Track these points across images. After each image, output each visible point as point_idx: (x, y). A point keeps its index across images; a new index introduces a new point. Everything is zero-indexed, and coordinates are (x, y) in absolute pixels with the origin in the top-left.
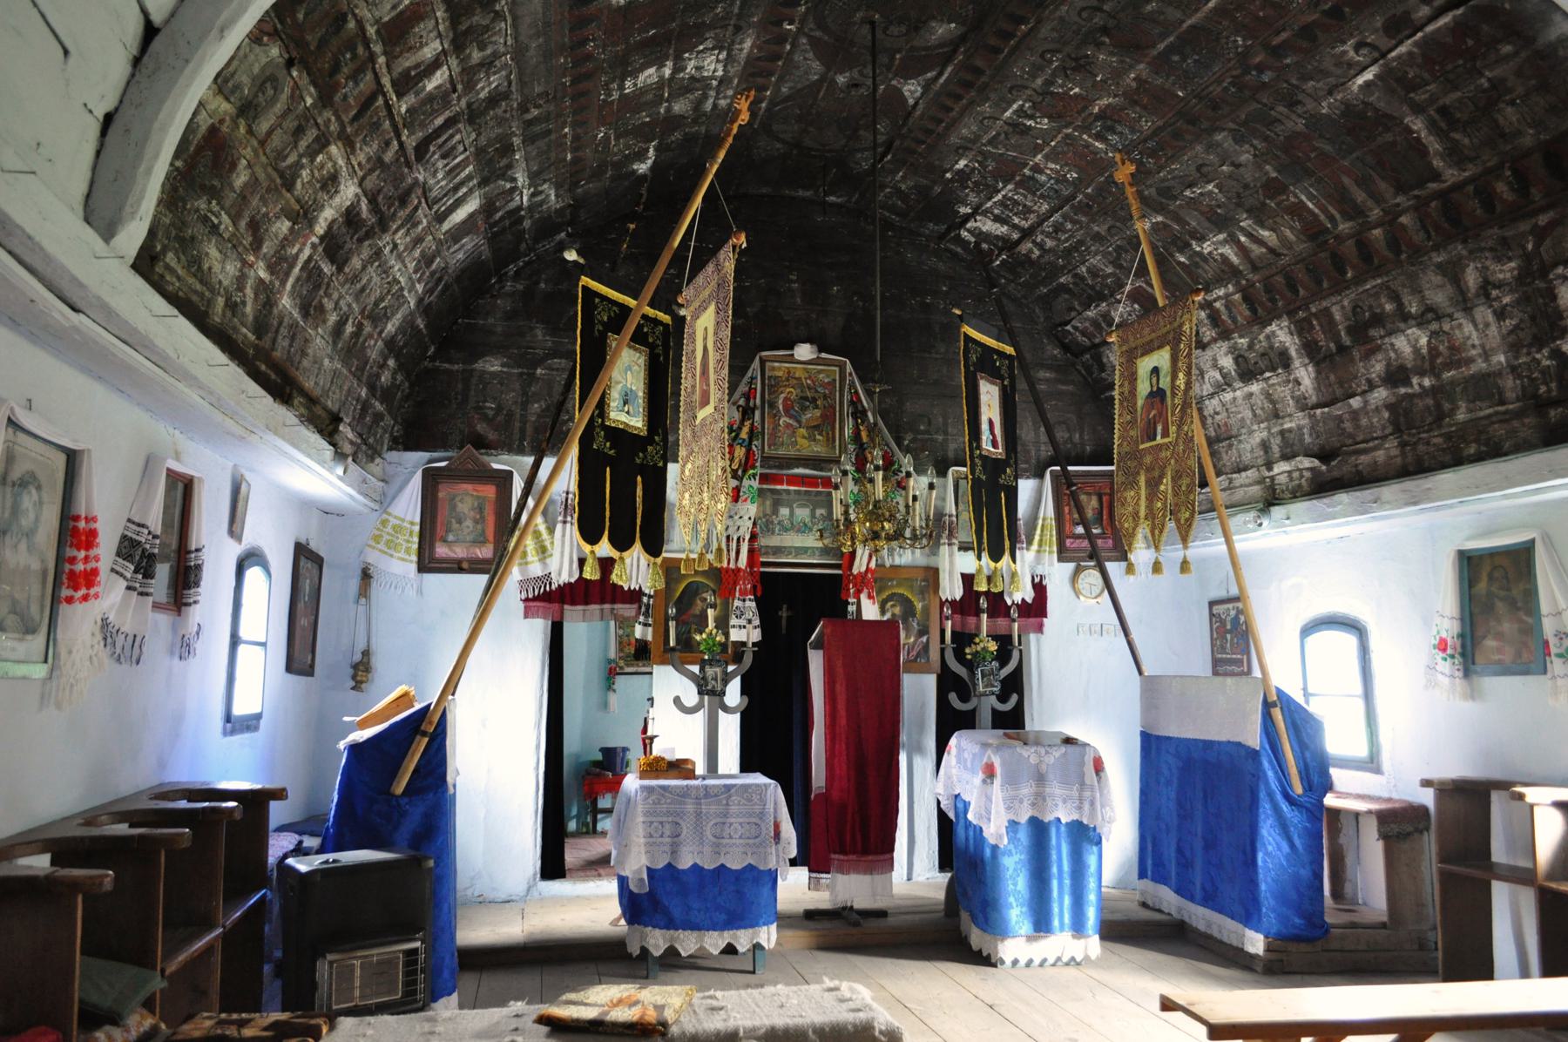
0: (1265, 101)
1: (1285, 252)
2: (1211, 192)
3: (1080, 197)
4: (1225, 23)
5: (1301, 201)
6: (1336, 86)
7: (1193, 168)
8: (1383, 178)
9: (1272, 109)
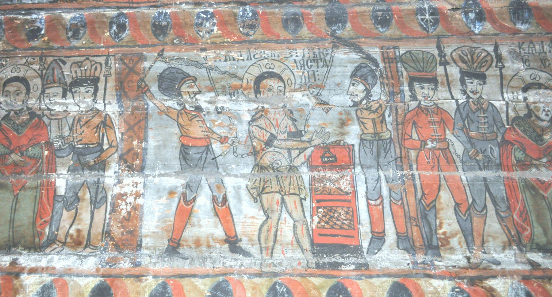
0: (448, 51)
1: (254, 250)
2: (234, 116)
3: (43, 15)
5: (355, 193)
6: (540, 86)
7: (256, 72)
8: (501, 219)
9: (445, 64)
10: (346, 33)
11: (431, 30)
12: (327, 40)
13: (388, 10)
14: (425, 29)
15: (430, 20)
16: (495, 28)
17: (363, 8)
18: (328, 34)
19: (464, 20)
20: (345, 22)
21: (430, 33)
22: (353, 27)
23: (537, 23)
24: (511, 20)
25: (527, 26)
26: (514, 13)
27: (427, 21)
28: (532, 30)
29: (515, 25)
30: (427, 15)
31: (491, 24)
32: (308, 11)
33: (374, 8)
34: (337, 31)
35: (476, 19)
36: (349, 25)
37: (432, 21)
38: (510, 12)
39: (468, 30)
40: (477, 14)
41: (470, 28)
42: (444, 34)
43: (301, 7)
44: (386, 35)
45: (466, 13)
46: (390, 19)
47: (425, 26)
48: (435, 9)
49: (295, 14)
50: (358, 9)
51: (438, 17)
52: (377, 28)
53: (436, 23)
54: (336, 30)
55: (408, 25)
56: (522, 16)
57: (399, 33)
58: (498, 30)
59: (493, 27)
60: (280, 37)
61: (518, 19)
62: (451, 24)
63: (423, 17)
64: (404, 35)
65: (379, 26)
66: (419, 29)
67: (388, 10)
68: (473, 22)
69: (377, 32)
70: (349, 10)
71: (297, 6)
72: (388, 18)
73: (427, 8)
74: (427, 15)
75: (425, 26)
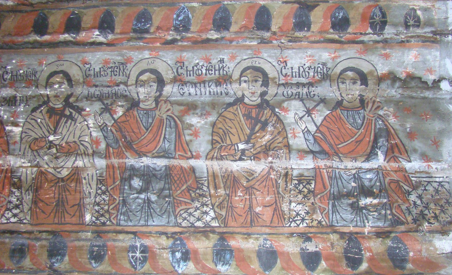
4: (221, 192)
10: (62, 266)
11: (138, 268)
12: (45, 272)
13: (104, 246)
14: (133, 266)
15: (140, 258)
16: (197, 268)
17: (81, 243)
18: (47, 266)
19: (171, 259)
20: (63, 256)
21: (137, 270)
22: (70, 260)
23: (237, 265)
24: (213, 261)
25: (227, 267)
26: (217, 255)
27: (136, 258)
28: (231, 272)
29: (216, 266)
30: (138, 252)
31: (194, 265)
32: (34, 242)
33: (91, 244)
34: (55, 264)
35: (182, 258)
36: (67, 258)
37: (142, 258)
38: (213, 253)
39: (173, 269)
40: (183, 253)
41: (174, 267)
42: (150, 272)
43: (29, 238)
44: (97, 270)
45: (173, 253)
46: (104, 255)
47: (134, 263)
48: (145, 247)
49: (23, 245)
50: (77, 243)
51: (147, 255)
52: (91, 263)
53: (144, 260)
54: (54, 262)
55: (119, 262)
56: (224, 258)
57: (109, 269)
58: (200, 271)
59: (195, 267)
60: (4, 266)
61: (220, 260)
62: (158, 262)
63: (134, 254)
64: (114, 271)
65: (93, 261)
66: (128, 266)
67: (104, 246)
68: (178, 262)
69: (89, 266)
70: (70, 244)
71: (25, 238)
72: (102, 253)
73: (139, 246)
74: (138, 252)
75: (134, 263)
